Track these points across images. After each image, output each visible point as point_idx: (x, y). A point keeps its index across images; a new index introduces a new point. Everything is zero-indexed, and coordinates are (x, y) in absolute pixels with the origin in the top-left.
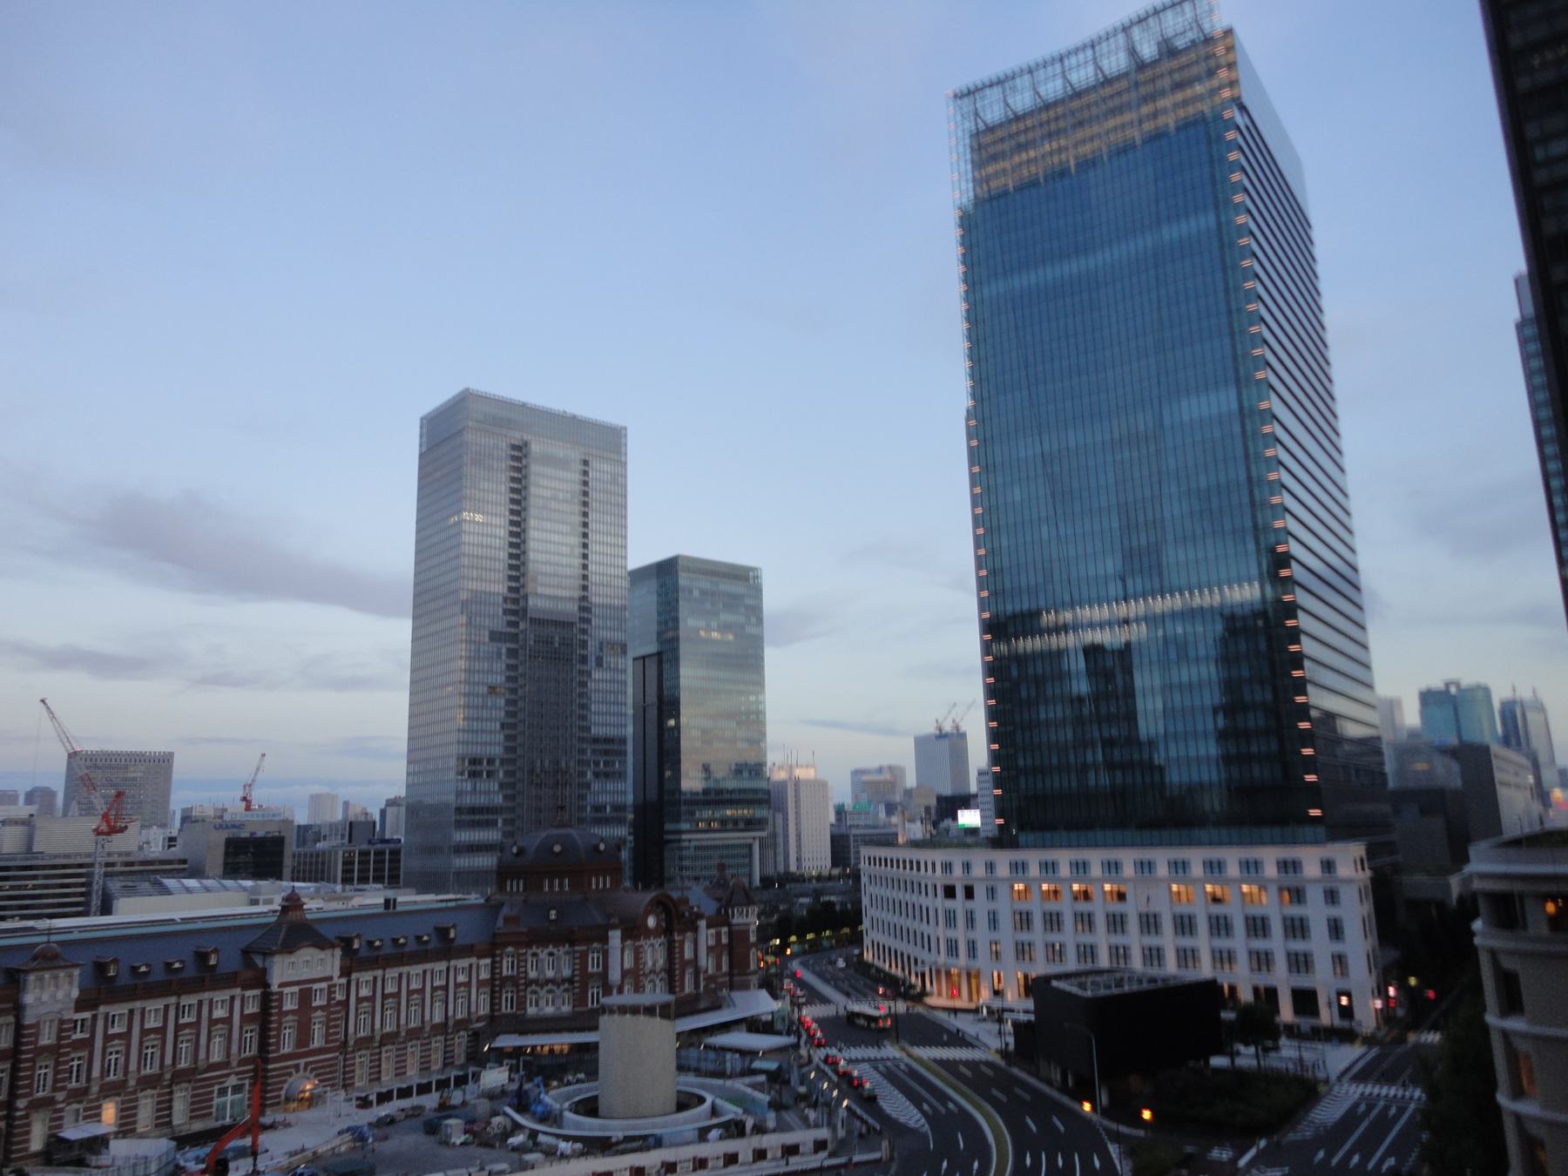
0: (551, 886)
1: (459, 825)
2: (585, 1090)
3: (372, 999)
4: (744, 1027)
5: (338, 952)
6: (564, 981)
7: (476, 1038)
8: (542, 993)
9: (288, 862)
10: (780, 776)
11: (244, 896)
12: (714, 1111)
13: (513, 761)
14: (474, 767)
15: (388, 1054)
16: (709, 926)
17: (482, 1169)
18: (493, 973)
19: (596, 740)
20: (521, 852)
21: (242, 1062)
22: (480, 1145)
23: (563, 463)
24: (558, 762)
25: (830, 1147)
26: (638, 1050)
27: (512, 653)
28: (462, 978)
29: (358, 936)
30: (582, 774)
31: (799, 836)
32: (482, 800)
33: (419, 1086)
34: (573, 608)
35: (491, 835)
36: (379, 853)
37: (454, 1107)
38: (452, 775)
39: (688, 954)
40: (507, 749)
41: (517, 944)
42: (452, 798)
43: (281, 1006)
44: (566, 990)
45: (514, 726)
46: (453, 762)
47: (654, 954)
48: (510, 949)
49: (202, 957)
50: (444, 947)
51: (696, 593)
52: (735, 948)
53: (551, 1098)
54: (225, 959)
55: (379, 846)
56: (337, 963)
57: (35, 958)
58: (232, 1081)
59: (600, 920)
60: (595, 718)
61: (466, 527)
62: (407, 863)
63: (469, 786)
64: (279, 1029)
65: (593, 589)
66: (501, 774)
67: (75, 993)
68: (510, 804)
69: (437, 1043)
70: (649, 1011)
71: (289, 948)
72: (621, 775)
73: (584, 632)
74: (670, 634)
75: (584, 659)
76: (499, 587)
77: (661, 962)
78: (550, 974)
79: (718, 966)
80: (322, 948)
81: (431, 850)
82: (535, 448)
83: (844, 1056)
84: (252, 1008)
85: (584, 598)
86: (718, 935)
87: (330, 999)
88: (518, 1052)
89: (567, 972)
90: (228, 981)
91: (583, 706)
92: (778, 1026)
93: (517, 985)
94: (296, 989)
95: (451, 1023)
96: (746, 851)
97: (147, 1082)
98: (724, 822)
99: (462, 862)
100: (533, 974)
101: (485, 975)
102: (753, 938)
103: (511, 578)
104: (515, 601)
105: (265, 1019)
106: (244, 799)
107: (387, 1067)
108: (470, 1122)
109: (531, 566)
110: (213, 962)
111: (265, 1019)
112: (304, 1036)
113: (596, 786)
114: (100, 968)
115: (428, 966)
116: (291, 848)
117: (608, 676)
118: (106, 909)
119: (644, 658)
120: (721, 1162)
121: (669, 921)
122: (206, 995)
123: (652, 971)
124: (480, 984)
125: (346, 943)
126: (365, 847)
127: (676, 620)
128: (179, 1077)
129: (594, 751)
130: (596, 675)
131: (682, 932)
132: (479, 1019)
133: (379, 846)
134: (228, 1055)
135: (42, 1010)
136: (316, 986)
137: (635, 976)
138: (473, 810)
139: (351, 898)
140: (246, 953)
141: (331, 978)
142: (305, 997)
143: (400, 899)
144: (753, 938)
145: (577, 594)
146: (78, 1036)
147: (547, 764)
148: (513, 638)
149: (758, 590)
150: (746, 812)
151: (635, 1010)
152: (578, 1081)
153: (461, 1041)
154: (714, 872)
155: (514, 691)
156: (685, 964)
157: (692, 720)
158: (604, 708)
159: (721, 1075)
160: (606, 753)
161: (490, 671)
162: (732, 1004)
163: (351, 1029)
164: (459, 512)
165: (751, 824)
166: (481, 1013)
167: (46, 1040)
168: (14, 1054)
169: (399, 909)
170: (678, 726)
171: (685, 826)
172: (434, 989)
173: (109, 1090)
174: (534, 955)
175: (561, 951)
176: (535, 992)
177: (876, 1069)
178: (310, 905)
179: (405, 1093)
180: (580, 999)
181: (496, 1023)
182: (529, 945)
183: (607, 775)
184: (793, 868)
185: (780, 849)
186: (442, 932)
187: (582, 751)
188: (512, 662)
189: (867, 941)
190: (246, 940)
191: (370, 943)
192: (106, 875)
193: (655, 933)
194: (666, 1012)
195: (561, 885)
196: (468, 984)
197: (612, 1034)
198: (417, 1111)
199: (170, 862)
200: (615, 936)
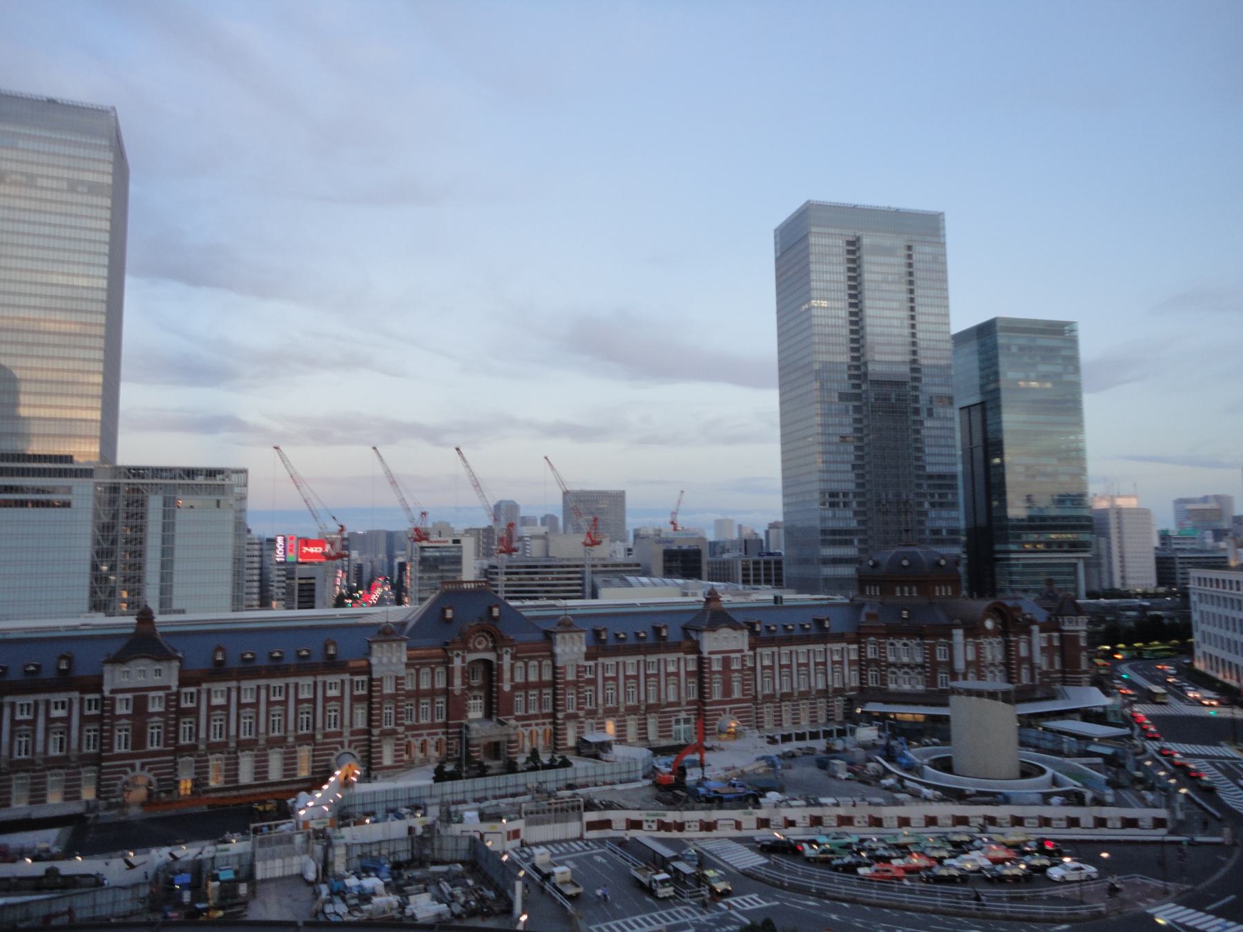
0: (902, 592)
1: (824, 543)
2: (941, 752)
3: (771, 668)
4: (1078, 716)
5: (746, 633)
6: (918, 666)
7: (850, 702)
8: (900, 674)
9: (705, 569)
10: (1102, 505)
11: (677, 590)
12: (1055, 782)
13: (863, 495)
14: (833, 499)
15: (786, 707)
16: (1042, 631)
17: (864, 800)
18: (860, 656)
19: (931, 477)
20: (876, 565)
21: (689, 703)
22: (860, 781)
23: (889, 251)
24: (898, 495)
25: (1170, 825)
26: (986, 728)
27: (857, 409)
28: (836, 658)
29: (759, 622)
30: (920, 504)
31: (1122, 557)
32: (841, 525)
33: (811, 733)
34: (906, 369)
35: (850, 551)
36: (767, 563)
37: (838, 752)
38: (816, 506)
39: (1023, 652)
40: (859, 485)
41: (877, 635)
42: (817, 524)
43: (710, 668)
44: (920, 673)
45: (861, 467)
46: (817, 495)
47: (993, 650)
48: (872, 639)
49: (657, 630)
50: (820, 633)
51: (1014, 350)
52: (1066, 649)
53: (913, 754)
54: (672, 633)
55: (766, 558)
56: (746, 640)
57: (559, 624)
58: (683, 715)
59: (943, 619)
60: (928, 459)
61: (815, 312)
62: (787, 571)
63: (830, 513)
64: (710, 683)
65: (921, 353)
66: (854, 504)
67: (584, 649)
68: (863, 528)
69: (821, 703)
70: (993, 695)
71: (713, 627)
72: (953, 505)
73: (915, 388)
74: (992, 386)
75: (917, 411)
76: (843, 357)
77: (999, 658)
78: (905, 660)
79: (1051, 664)
80: (735, 629)
81: (805, 561)
82: (866, 241)
83: (1178, 750)
84: (692, 667)
85: (914, 361)
86: (1050, 639)
87: (743, 665)
88: (883, 717)
89: (919, 660)
90: (675, 647)
91: (919, 450)
92: (1112, 719)
93: (878, 665)
94: (719, 656)
95: (830, 690)
96: (1071, 569)
97: (632, 710)
98: (1049, 544)
99: (828, 571)
100: (891, 659)
101: (854, 657)
102: (1083, 643)
103: (853, 350)
104: (857, 368)
105: (700, 674)
106: (672, 523)
107: (787, 717)
108: (851, 763)
109: (869, 339)
110: (664, 633)
111: (700, 674)
112: (727, 690)
113: (933, 514)
114: (597, 633)
115: (811, 647)
116: (706, 558)
117: (938, 424)
118: (594, 595)
119: (969, 407)
120: (1064, 824)
121: (1005, 624)
122: (662, 656)
123: (992, 664)
124: (851, 663)
125: (751, 626)
126: (756, 558)
127: (996, 373)
128: (650, 708)
129: (929, 486)
130: (928, 423)
131: (1016, 634)
132: (852, 689)
133: (766, 558)
134: (679, 697)
135: (566, 658)
136: (733, 655)
137: (977, 667)
138: (834, 532)
139: (749, 594)
140: (685, 629)
141: (742, 651)
142: (726, 662)
143: (785, 597)
144: (1083, 643)
145: (908, 358)
146: (588, 676)
147: (890, 496)
148: (858, 397)
149: (1074, 342)
150: (1069, 536)
151: (979, 694)
152: (935, 744)
153: (839, 703)
154: (1044, 586)
155: (860, 439)
156: (1021, 660)
157: (1016, 461)
158: (936, 450)
159: (1059, 753)
160: (940, 486)
161: (841, 425)
162: (1065, 696)
163: (759, 688)
164: (809, 301)
165: (1075, 546)
166: (853, 684)
167: (571, 677)
168: (553, 684)
169: (785, 604)
170: (1002, 465)
171: (1013, 547)
172: (816, 664)
173: (611, 713)
174: (892, 644)
175: (913, 643)
176: (894, 673)
177: (1213, 764)
178: (724, 598)
179: (801, 737)
180: (932, 681)
181: (865, 694)
182: (887, 636)
183: (941, 505)
184: (1117, 585)
185: (1105, 569)
186: (819, 623)
187: (919, 486)
188: (857, 416)
189: (1198, 652)
190: (685, 620)
191: (768, 628)
192: (593, 572)
193: (992, 633)
194: (1007, 698)
195: (910, 592)
196: (841, 663)
197: (959, 710)
198: (810, 751)
199: (629, 565)
200: (958, 634)
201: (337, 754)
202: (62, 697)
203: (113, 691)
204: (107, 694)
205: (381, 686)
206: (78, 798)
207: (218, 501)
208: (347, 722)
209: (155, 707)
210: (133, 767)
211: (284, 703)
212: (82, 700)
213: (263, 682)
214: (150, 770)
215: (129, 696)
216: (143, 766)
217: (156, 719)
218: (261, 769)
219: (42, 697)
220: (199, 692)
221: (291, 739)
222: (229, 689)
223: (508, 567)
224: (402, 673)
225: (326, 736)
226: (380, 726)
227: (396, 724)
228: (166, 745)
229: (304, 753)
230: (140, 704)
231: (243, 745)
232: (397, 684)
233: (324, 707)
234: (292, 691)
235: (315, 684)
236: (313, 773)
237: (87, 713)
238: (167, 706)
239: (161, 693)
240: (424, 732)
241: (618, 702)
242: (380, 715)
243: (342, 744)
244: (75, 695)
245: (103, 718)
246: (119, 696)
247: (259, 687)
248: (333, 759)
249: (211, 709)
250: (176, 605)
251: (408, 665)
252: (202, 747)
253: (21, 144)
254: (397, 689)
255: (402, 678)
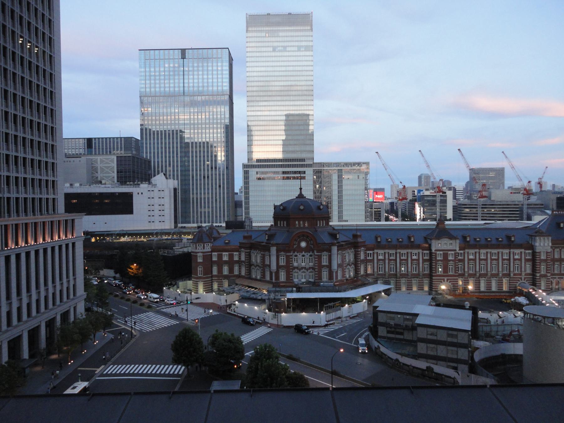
57: (536, 233)
106: (539, 183)
118: (529, 219)
192: (528, 208)
199: (537, 205)
201: (519, 282)
202: (415, 251)
203: (436, 250)
204: (433, 251)
205: (540, 255)
206: (423, 290)
207: (358, 176)
208: (523, 270)
209: (450, 258)
210: (444, 280)
211: (498, 260)
212: (423, 253)
213: (489, 250)
214: (450, 282)
215: (442, 252)
216: (448, 280)
217: (451, 262)
218: (489, 286)
219: (409, 251)
220: (464, 253)
221: (501, 275)
222: (476, 252)
223: (483, 205)
224: (549, 251)
225: (514, 275)
226: (540, 273)
227: (547, 272)
228: (455, 273)
229: (505, 281)
230: (446, 256)
231: (481, 276)
232: (547, 255)
233: (514, 263)
234: (500, 255)
235: (510, 252)
236: (510, 289)
237: (424, 258)
238: (455, 258)
239: (453, 252)
240: (557, 277)
241: (487, 271)
242: (540, 268)
243: (521, 278)
244: (420, 251)
245: (431, 260)
246: (438, 252)
247: (487, 252)
248: (518, 284)
249: (469, 260)
250: (344, 218)
251: (551, 247)
252: (466, 275)
253: (281, 34)
254: (547, 257)
255: (549, 253)
